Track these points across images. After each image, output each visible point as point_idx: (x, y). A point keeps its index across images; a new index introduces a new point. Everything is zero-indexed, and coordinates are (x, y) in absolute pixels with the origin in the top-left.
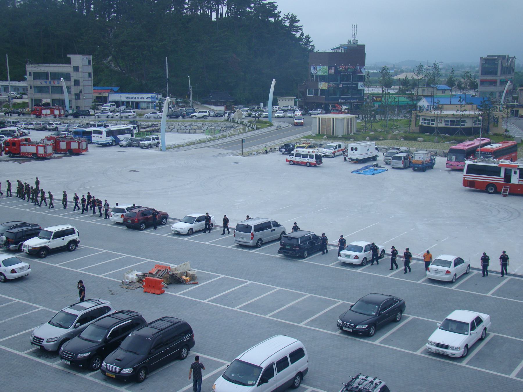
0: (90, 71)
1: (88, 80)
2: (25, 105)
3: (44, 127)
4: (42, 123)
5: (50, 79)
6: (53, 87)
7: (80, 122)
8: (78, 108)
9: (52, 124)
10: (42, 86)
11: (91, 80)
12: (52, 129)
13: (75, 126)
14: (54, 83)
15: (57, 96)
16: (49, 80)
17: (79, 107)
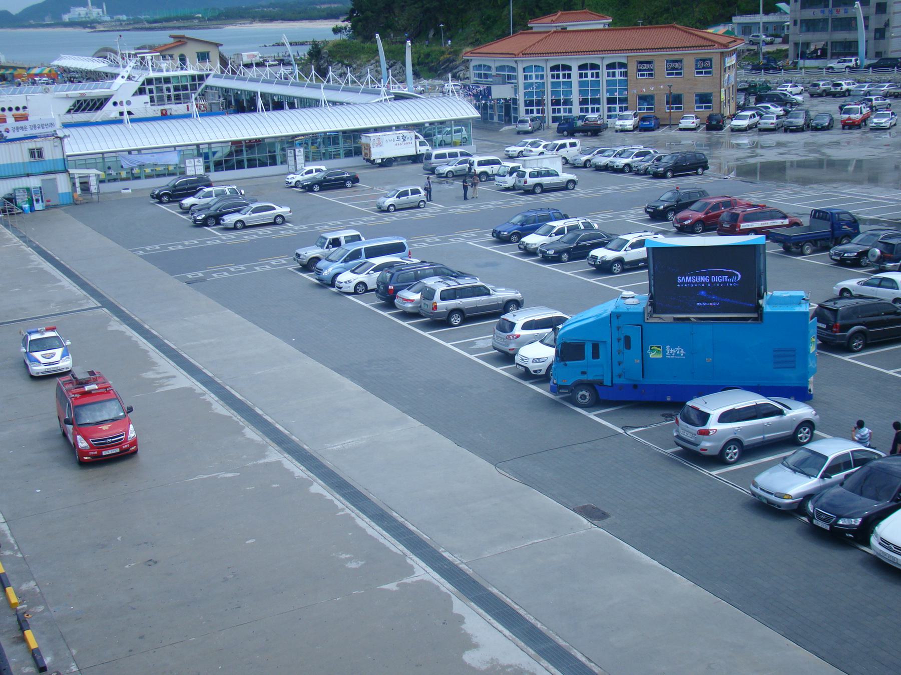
2: (784, 54)
3: (824, 91)
4: (821, 83)
6: (835, 20)
7: (890, 79)
8: (878, 54)
9: (840, 85)
10: (814, 20)
12: (839, 93)
13: (884, 87)
14: (838, 12)
15: (841, 36)
17: (881, 53)
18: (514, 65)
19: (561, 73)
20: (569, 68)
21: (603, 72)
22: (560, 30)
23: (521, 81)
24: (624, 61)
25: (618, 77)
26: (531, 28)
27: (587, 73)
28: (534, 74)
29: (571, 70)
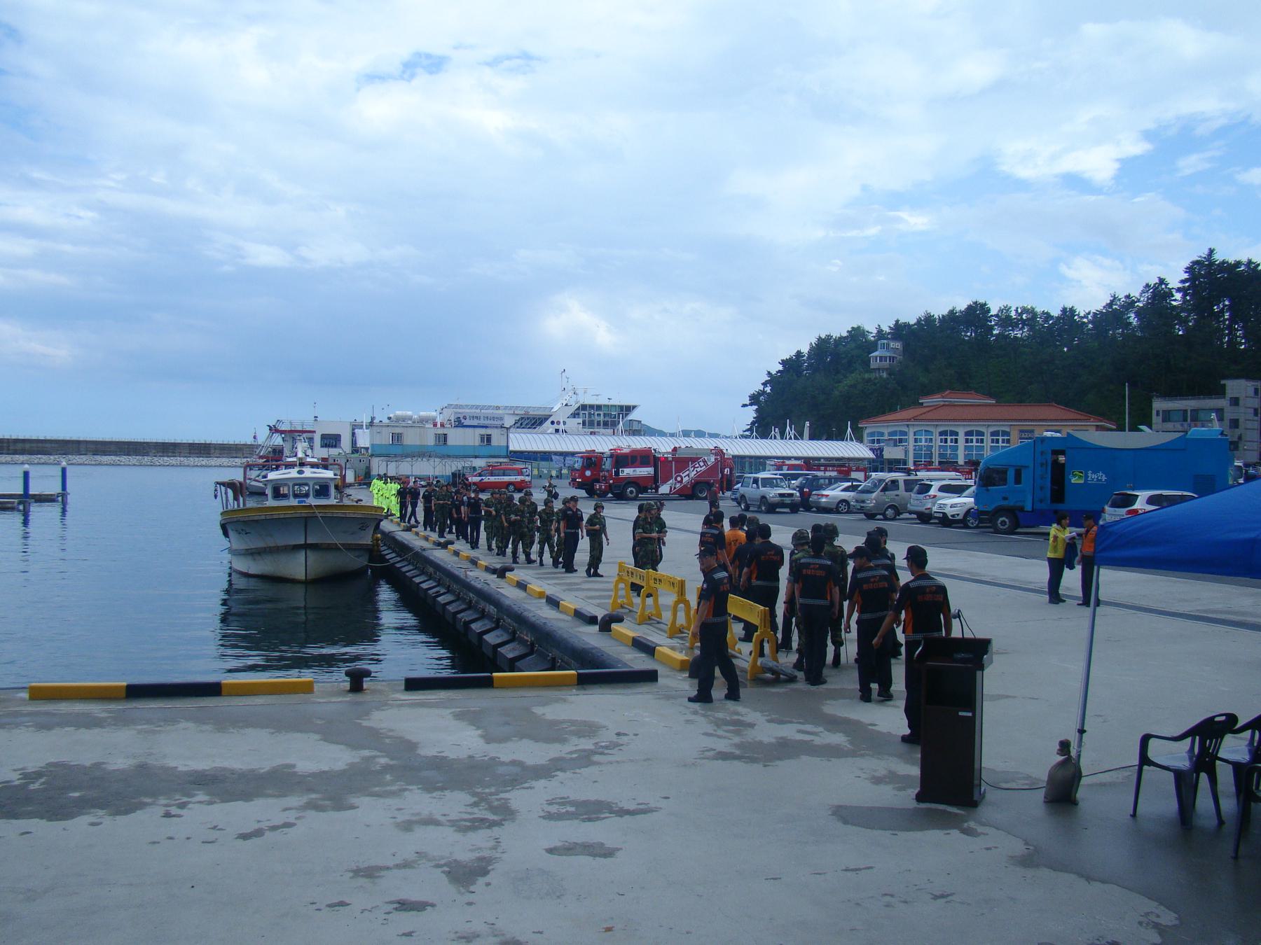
0: (1256, 406)
1: (1254, 421)
5: (1189, 420)
11: (1257, 421)
16: (1187, 421)
18: (905, 429)
19: (949, 438)
20: (956, 434)
21: (987, 438)
22: (947, 403)
23: (912, 442)
24: (1007, 429)
25: (1000, 444)
26: (922, 403)
27: (972, 439)
28: (923, 438)
29: (958, 436)
